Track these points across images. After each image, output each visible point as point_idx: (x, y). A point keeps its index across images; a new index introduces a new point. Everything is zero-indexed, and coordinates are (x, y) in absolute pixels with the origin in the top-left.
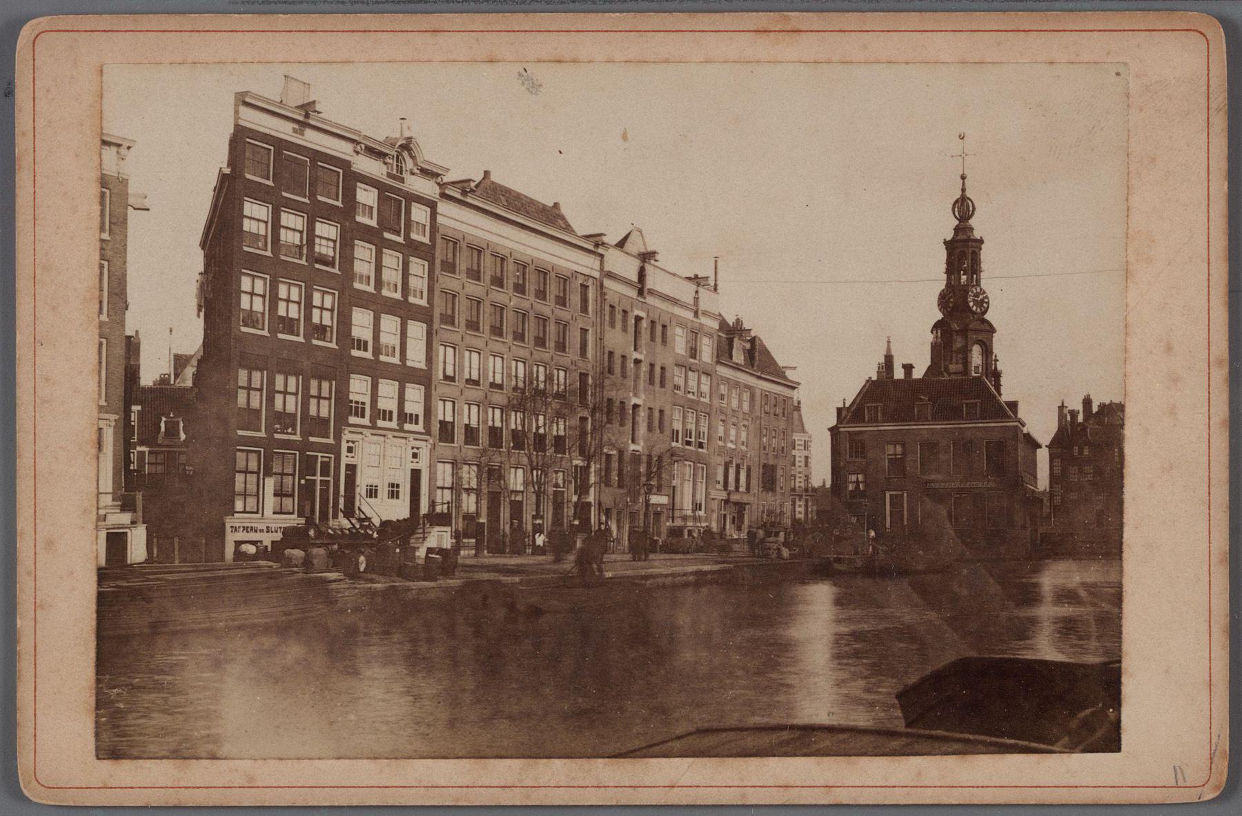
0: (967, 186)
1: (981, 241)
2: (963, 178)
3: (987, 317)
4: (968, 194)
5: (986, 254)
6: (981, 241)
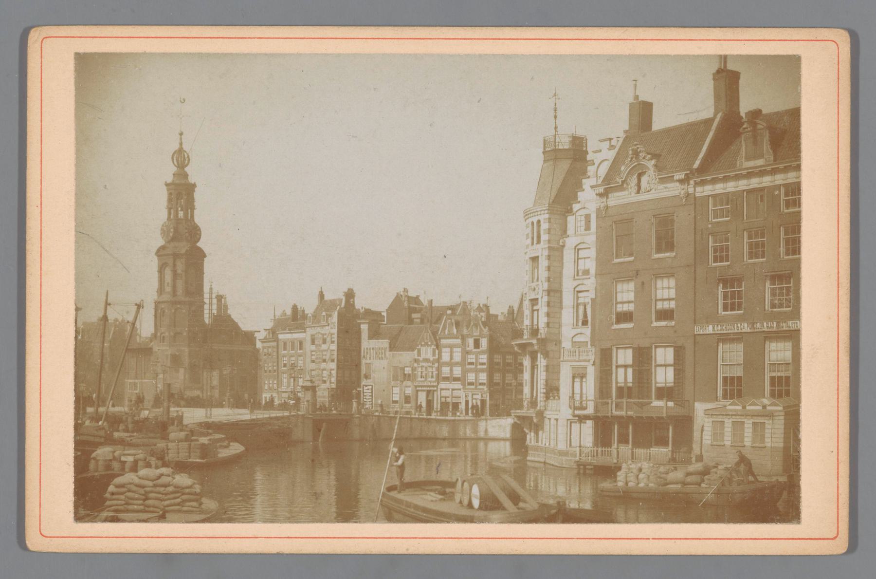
1: (194, 185)
3: (199, 244)
5: (197, 195)
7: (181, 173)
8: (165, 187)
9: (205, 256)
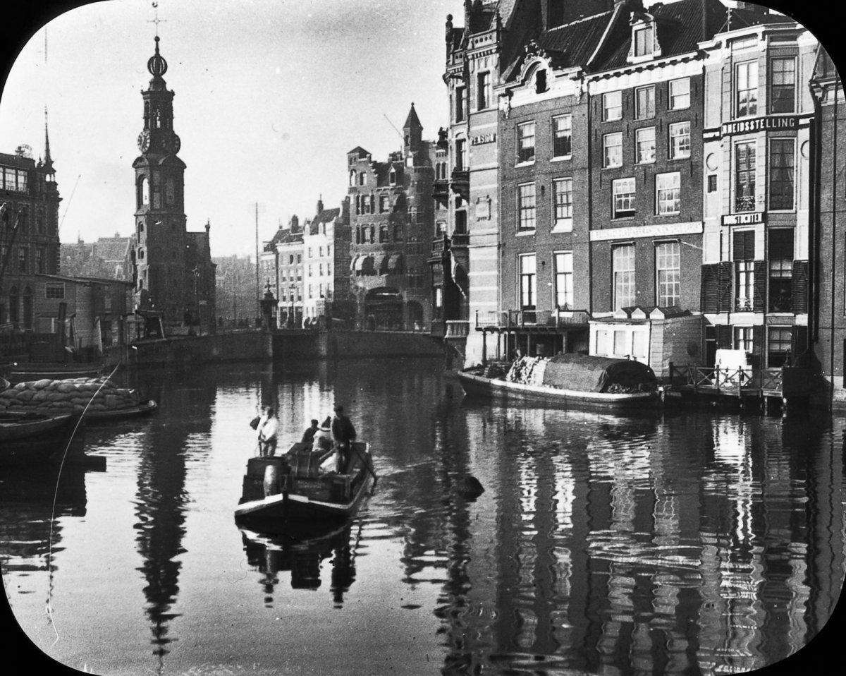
0: (160, 47)
1: (172, 93)
2: (157, 39)
4: (162, 53)
5: (176, 104)
6: (172, 93)
7: (158, 82)
8: (141, 96)
9: (185, 167)
